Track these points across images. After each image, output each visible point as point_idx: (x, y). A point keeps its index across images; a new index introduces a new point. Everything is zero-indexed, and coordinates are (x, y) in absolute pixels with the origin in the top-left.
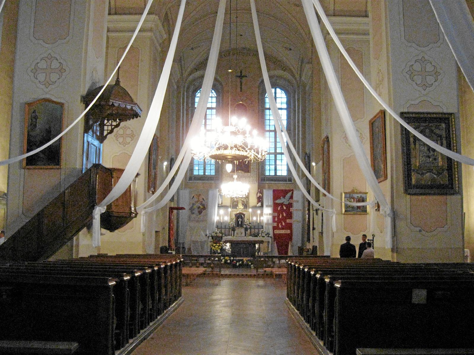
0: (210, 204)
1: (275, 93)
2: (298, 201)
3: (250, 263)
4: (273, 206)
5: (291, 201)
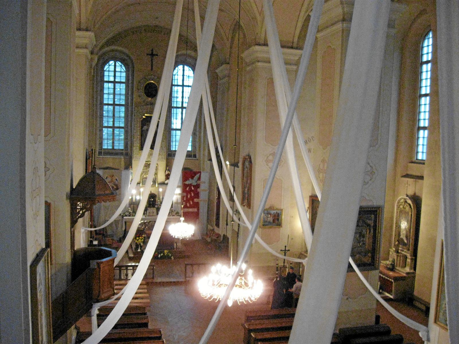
0: (122, 185)
1: (184, 70)
2: (205, 183)
3: (170, 255)
5: (199, 182)
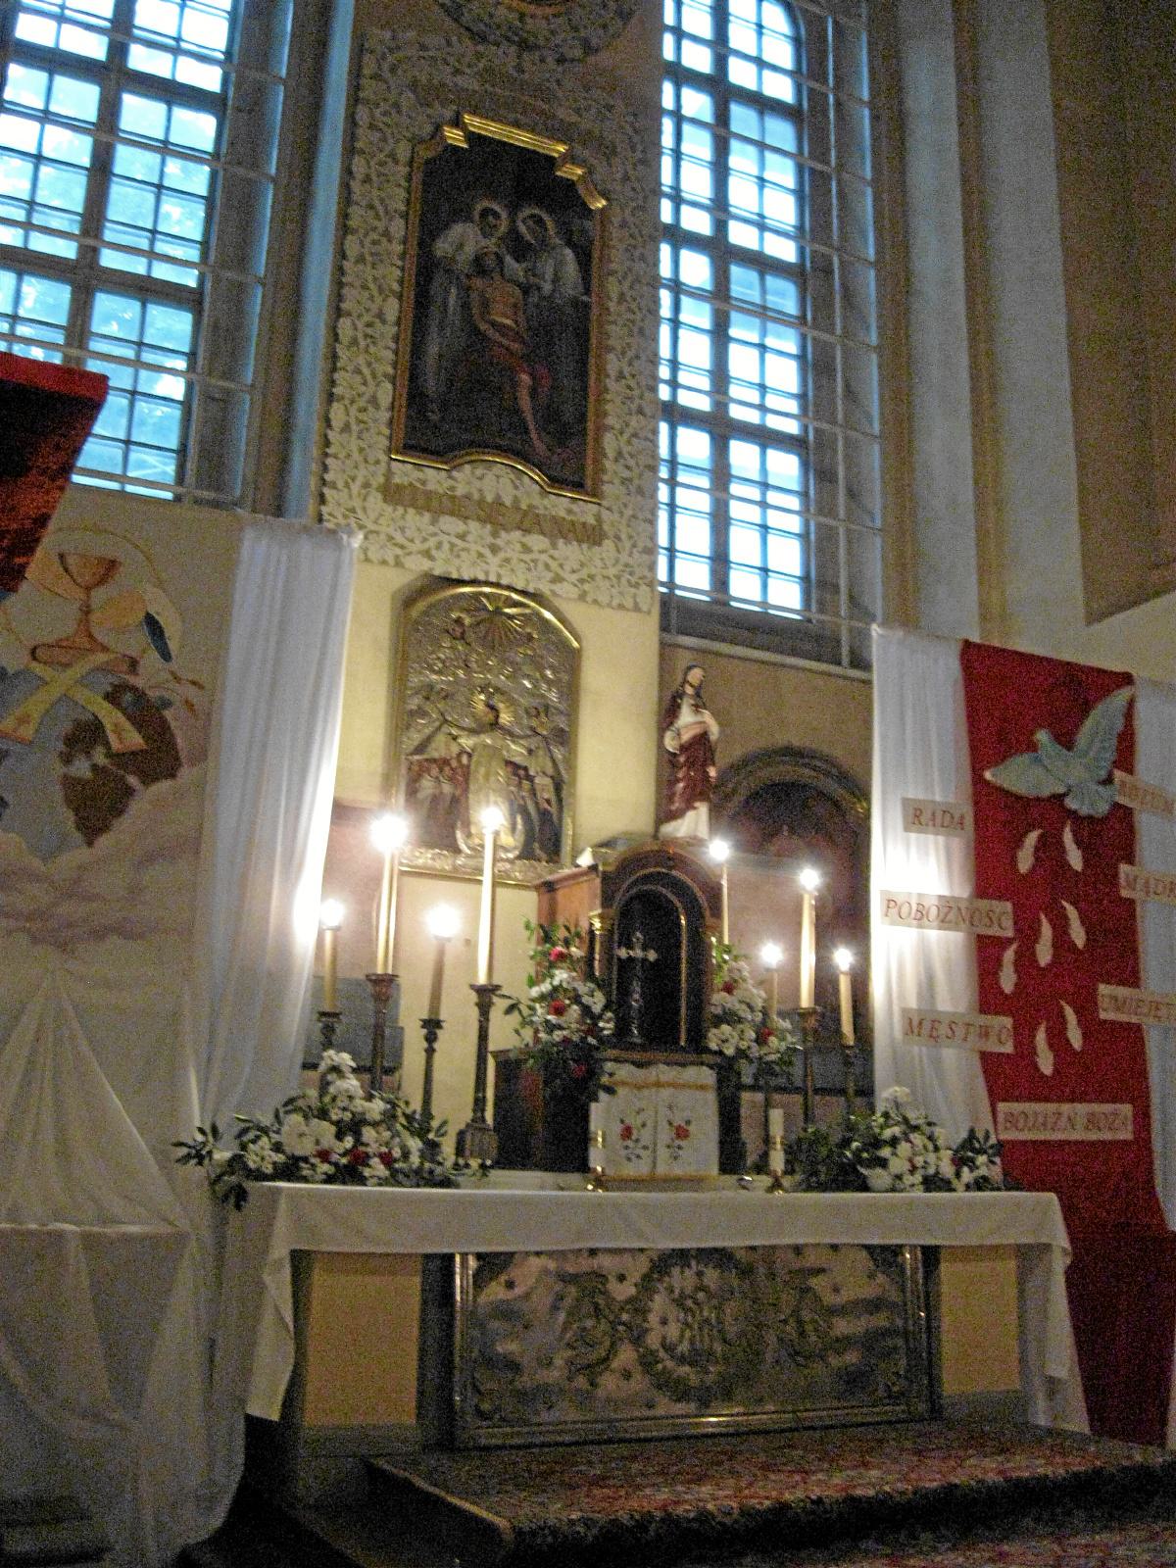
4: (969, 820)
